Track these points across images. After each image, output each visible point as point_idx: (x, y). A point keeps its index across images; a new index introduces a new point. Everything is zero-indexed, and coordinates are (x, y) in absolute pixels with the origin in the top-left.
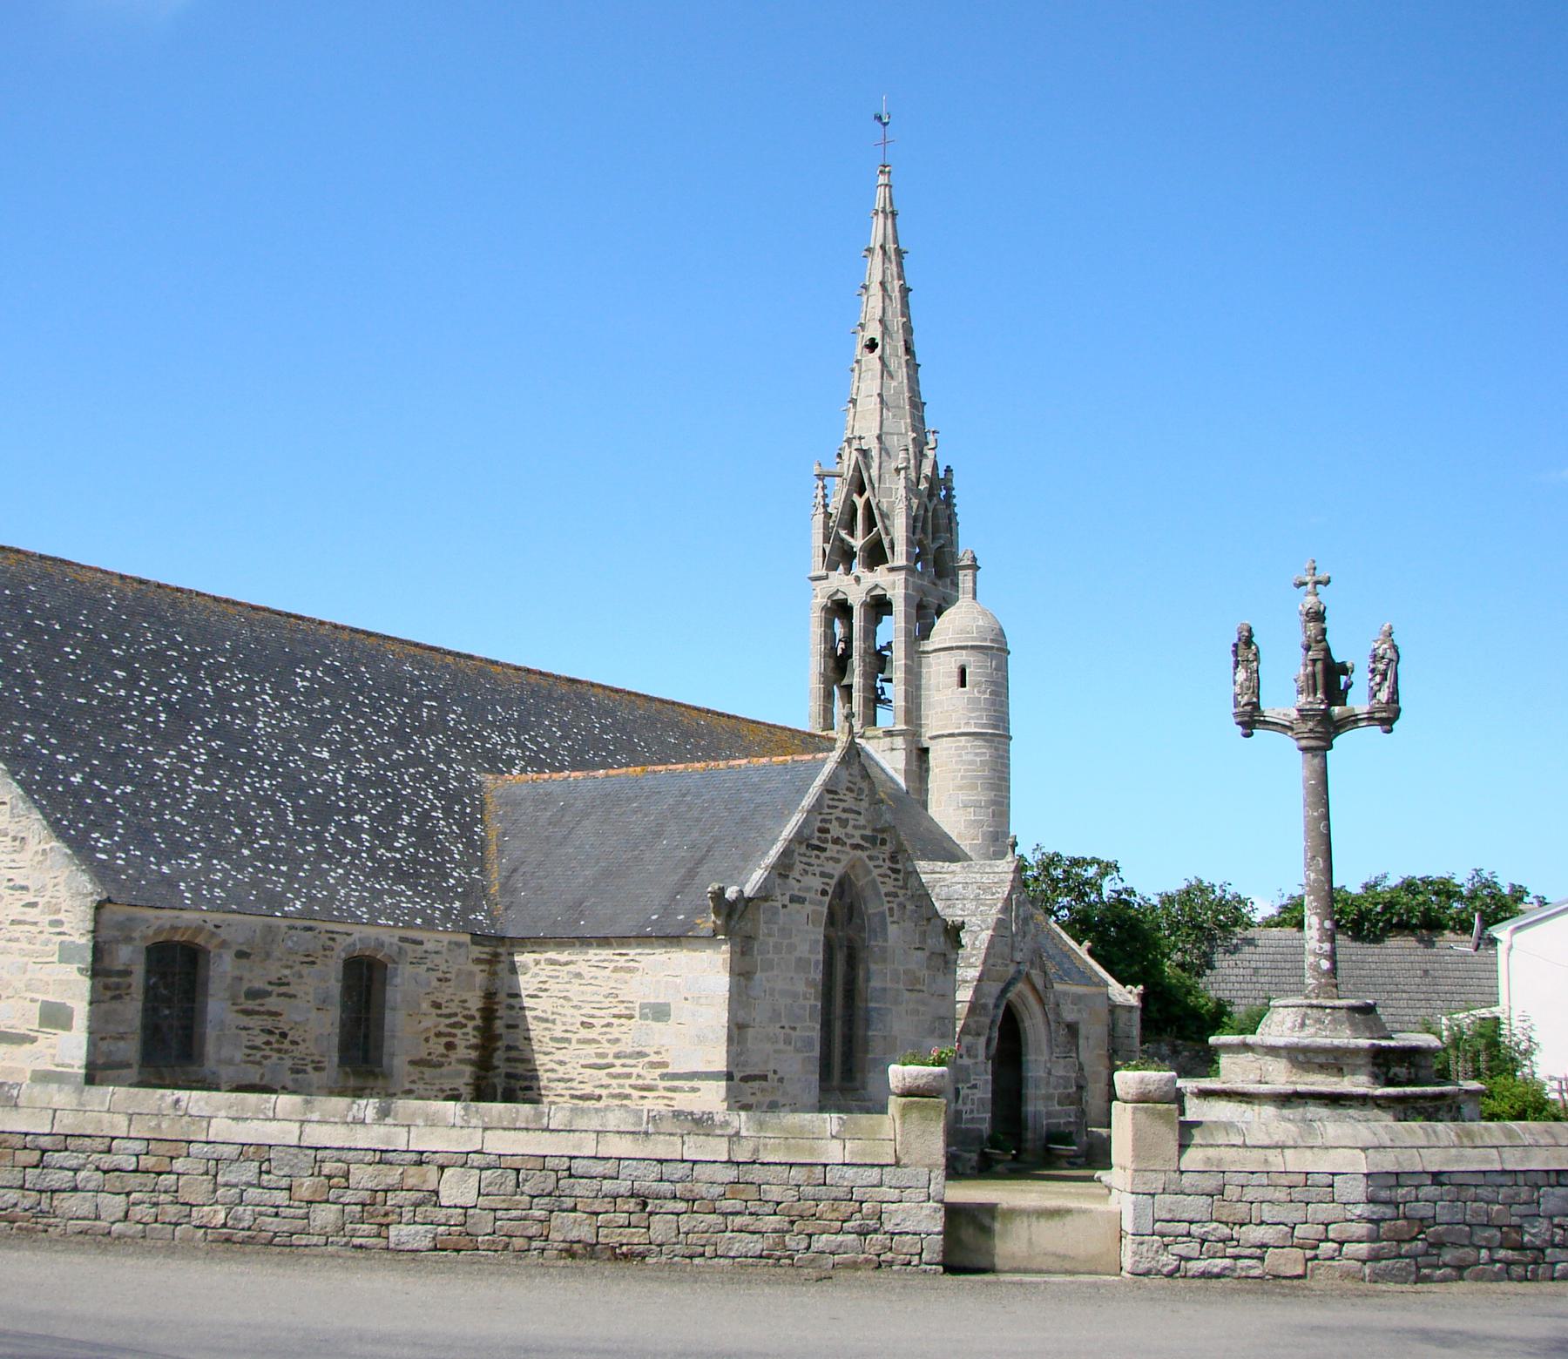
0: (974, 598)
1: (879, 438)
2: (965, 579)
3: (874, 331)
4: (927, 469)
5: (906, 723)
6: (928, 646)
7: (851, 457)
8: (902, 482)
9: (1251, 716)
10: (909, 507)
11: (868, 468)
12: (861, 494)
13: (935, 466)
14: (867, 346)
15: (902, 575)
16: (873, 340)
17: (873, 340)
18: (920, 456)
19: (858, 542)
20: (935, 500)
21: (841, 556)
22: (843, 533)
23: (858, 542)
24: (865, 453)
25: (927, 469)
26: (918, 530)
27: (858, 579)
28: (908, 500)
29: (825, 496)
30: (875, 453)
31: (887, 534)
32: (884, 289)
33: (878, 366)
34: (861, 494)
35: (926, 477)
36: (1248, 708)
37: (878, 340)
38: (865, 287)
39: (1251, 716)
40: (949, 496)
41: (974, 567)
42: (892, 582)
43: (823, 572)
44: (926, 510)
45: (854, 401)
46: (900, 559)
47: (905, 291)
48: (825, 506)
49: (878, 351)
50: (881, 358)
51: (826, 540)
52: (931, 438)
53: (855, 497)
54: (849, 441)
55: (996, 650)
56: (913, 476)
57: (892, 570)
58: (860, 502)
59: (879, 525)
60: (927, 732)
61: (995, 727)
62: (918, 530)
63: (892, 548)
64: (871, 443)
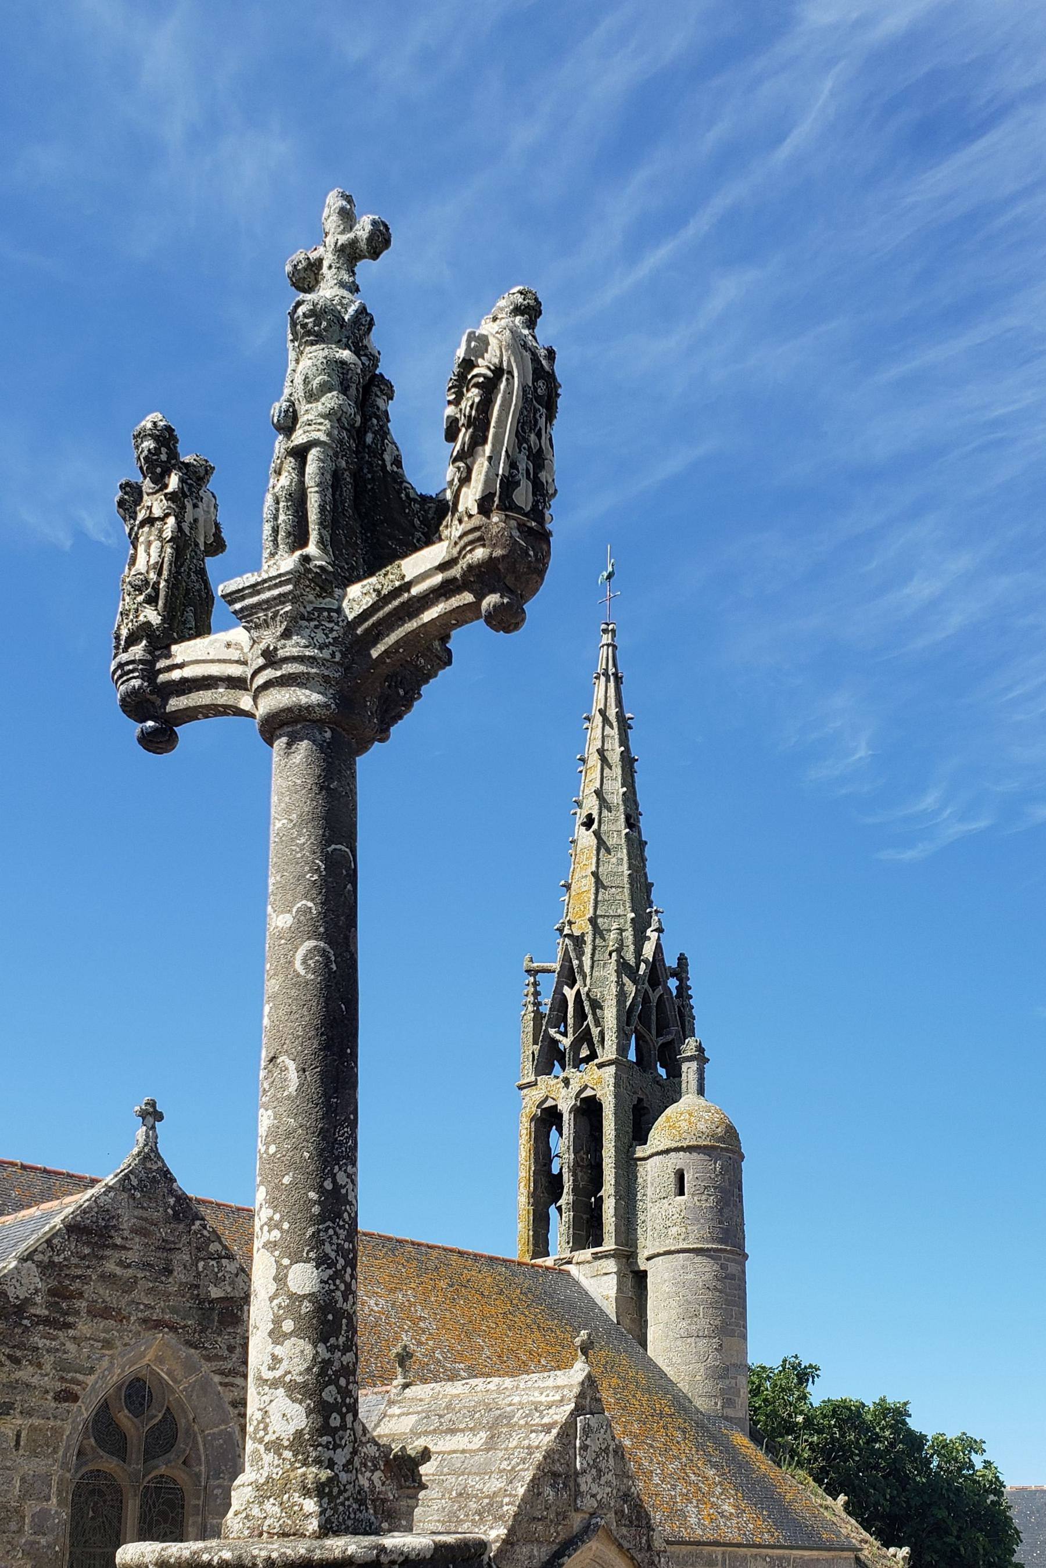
0: (701, 1091)
1: (593, 921)
2: (689, 1071)
3: (591, 805)
4: (648, 950)
5: (616, 1244)
6: (640, 1152)
7: (561, 945)
8: (613, 966)
9: (150, 672)
10: (621, 995)
11: (579, 958)
12: (572, 988)
13: (659, 946)
14: (583, 824)
15: (612, 1069)
16: (589, 816)
17: (589, 816)
18: (640, 939)
19: (566, 1042)
20: (660, 990)
21: (550, 1057)
22: (552, 1031)
23: (566, 1042)
24: (578, 942)
25: (648, 950)
26: (635, 1020)
27: (567, 1082)
28: (620, 984)
29: (536, 994)
30: (589, 939)
31: (598, 1023)
32: (604, 760)
33: (594, 841)
34: (572, 988)
35: (646, 961)
36: (138, 651)
37: (596, 816)
38: (583, 760)
39: (150, 672)
40: (683, 989)
41: (701, 1057)
42: (601, 1081)
43: (533, 1078)
44: (646, 999)
45: (568, 887)
46: (609, 1051)
47: (628, 762)
48: (537, 1004)
49: (595, 826)
50: (597, 834)
51: (535, 1042)
52: (655, 918)
53: (566, 990)
54: (560, 930)
55: (724, 1151)
56: (632, 962)
57: (600, 1066)
58: (570, 994)
59: (590, 1018)
60: (643, 1254)
61: (721, 1241)
62: (635, 1020)
63: (602, 1041)
64: (582, 927)
